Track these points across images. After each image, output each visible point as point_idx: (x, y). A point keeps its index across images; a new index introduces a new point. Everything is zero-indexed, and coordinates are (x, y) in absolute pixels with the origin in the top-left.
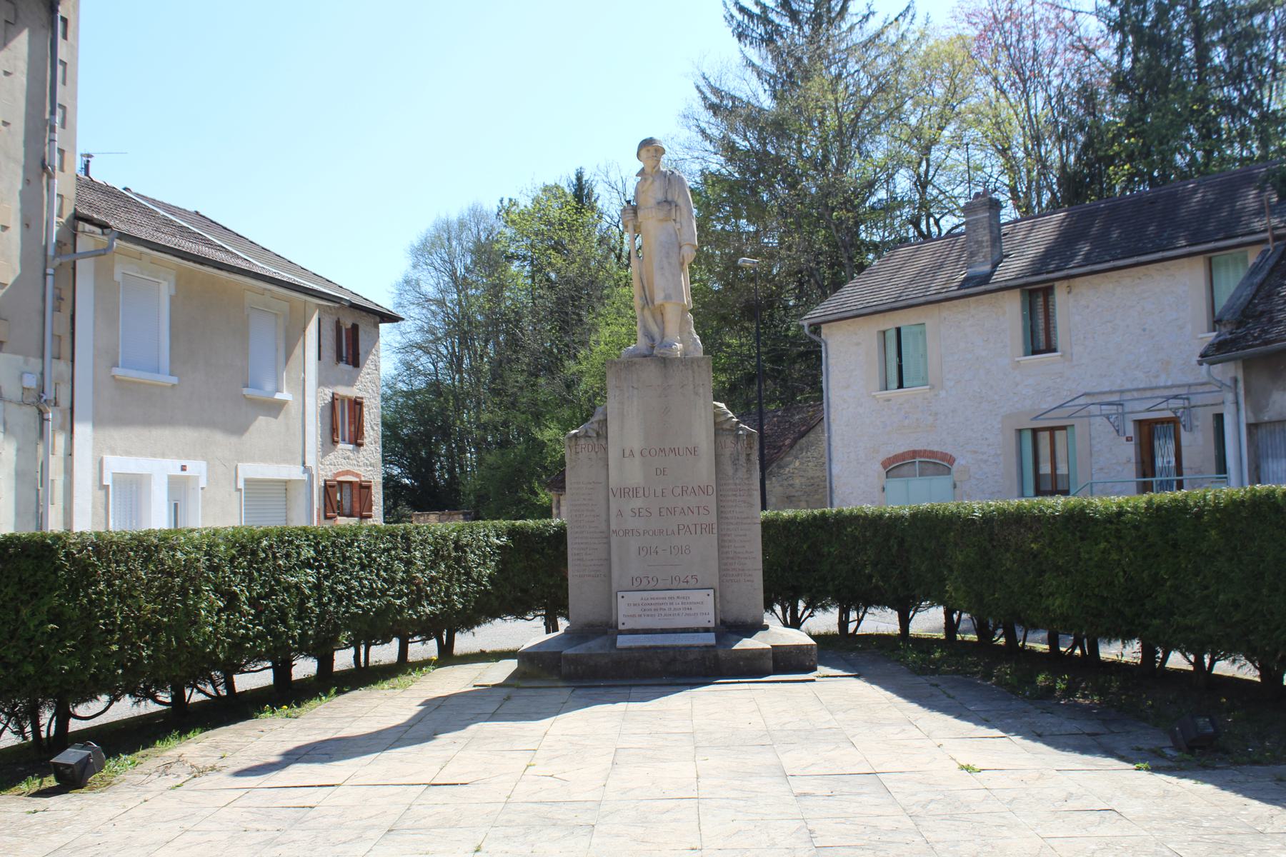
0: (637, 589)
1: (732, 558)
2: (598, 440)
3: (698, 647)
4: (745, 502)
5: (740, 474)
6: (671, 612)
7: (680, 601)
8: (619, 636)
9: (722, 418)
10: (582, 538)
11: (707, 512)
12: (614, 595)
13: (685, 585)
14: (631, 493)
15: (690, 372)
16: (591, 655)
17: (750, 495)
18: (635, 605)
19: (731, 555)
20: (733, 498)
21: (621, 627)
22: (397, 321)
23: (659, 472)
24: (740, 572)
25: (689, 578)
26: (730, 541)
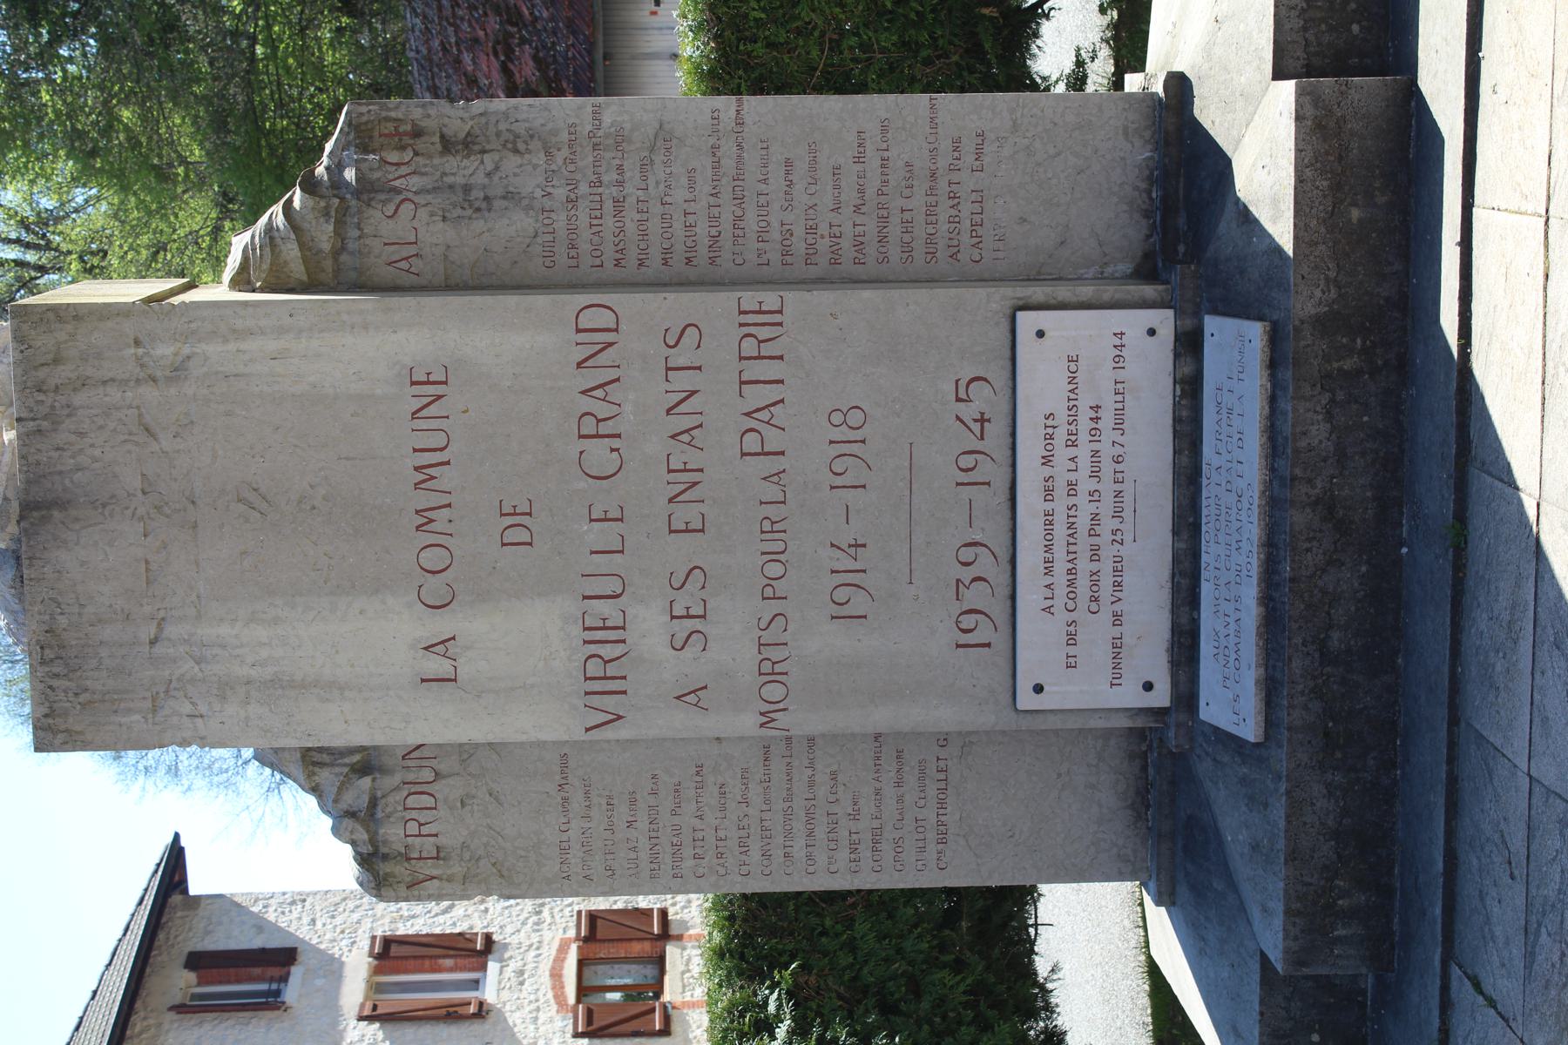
0: (1005, 629)
1: (884, 220)
2: (384, 771)
3: (1273, 400)
4: (645, 166)
5: (529, 184)
6: (1107, 488)
7: (1062, 454)
8: (1205, 714)
9: (291, 251)
10: (788, 834)
11: (691, 335)
12: (1026, 723)
13: (996, 429)
14: (607, 651)
15: (79, 399)
16: (1292, 856)
17: (620, 140)
18: (1072, 639)
19: (871, 227)
20: (631, 216)
21: (1161, 697)
22: (181, 850)
23: (522, 535)
24: (942, 185)
25: (969, 412)
26: (811, 230)
